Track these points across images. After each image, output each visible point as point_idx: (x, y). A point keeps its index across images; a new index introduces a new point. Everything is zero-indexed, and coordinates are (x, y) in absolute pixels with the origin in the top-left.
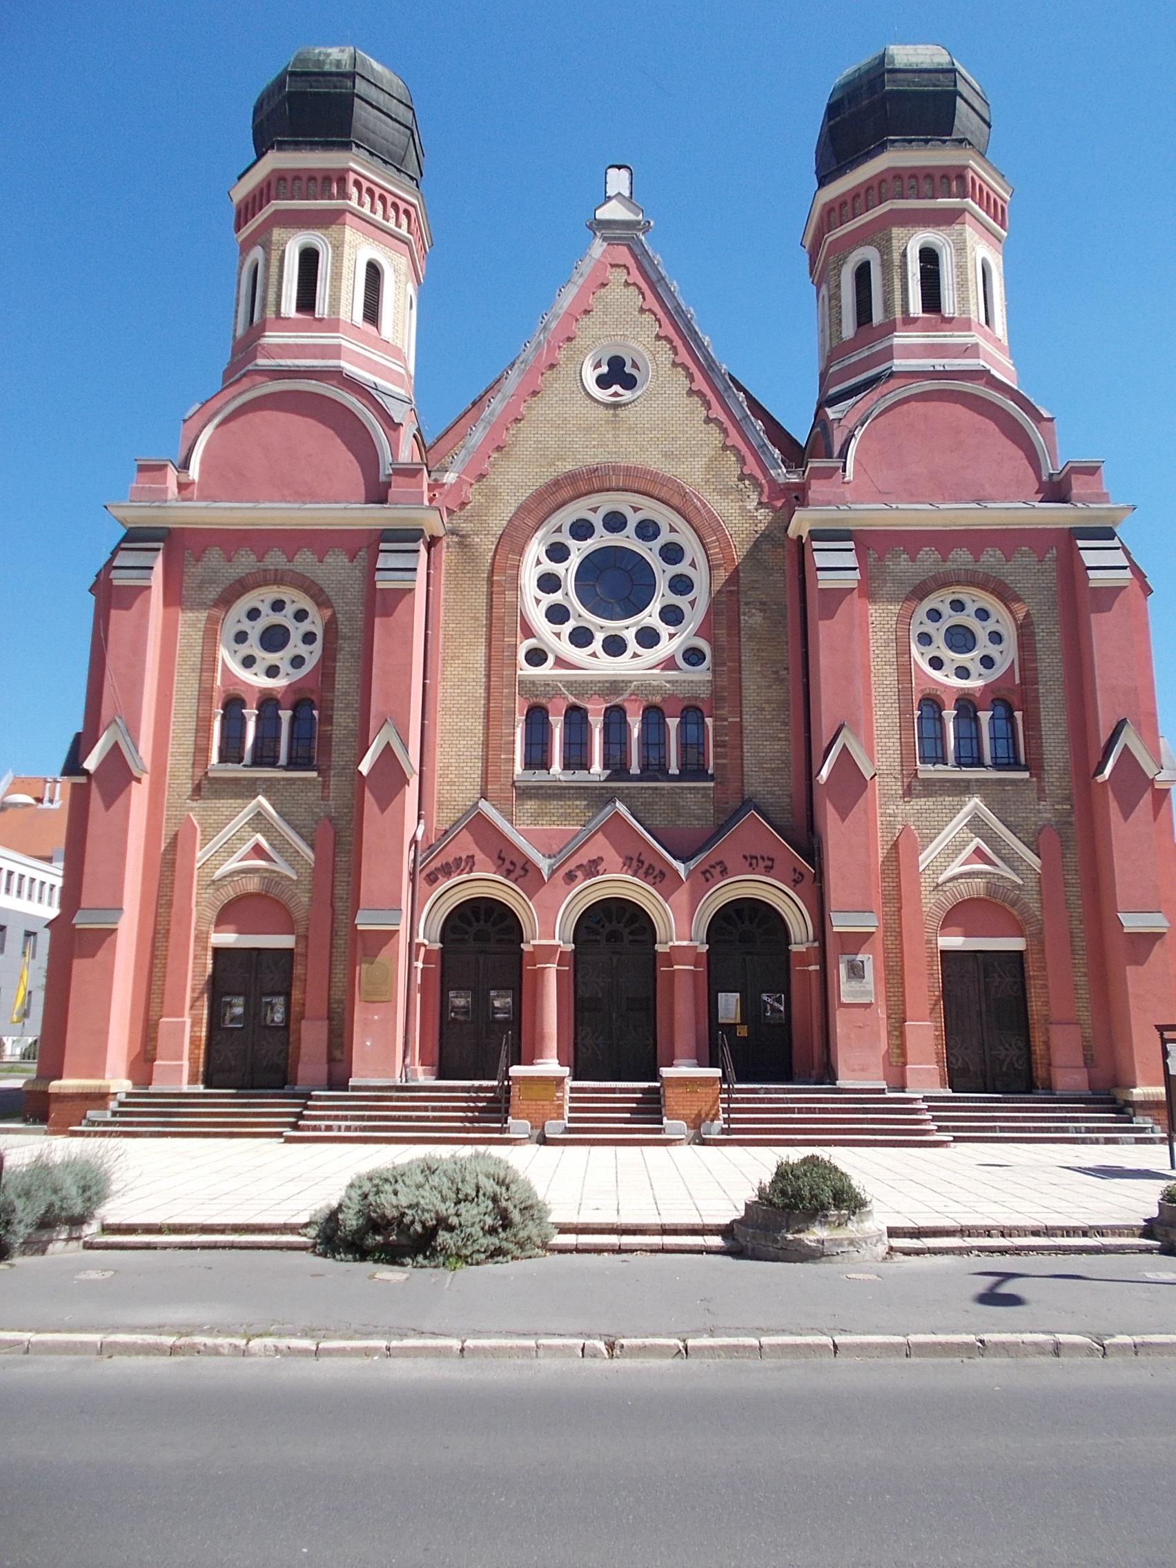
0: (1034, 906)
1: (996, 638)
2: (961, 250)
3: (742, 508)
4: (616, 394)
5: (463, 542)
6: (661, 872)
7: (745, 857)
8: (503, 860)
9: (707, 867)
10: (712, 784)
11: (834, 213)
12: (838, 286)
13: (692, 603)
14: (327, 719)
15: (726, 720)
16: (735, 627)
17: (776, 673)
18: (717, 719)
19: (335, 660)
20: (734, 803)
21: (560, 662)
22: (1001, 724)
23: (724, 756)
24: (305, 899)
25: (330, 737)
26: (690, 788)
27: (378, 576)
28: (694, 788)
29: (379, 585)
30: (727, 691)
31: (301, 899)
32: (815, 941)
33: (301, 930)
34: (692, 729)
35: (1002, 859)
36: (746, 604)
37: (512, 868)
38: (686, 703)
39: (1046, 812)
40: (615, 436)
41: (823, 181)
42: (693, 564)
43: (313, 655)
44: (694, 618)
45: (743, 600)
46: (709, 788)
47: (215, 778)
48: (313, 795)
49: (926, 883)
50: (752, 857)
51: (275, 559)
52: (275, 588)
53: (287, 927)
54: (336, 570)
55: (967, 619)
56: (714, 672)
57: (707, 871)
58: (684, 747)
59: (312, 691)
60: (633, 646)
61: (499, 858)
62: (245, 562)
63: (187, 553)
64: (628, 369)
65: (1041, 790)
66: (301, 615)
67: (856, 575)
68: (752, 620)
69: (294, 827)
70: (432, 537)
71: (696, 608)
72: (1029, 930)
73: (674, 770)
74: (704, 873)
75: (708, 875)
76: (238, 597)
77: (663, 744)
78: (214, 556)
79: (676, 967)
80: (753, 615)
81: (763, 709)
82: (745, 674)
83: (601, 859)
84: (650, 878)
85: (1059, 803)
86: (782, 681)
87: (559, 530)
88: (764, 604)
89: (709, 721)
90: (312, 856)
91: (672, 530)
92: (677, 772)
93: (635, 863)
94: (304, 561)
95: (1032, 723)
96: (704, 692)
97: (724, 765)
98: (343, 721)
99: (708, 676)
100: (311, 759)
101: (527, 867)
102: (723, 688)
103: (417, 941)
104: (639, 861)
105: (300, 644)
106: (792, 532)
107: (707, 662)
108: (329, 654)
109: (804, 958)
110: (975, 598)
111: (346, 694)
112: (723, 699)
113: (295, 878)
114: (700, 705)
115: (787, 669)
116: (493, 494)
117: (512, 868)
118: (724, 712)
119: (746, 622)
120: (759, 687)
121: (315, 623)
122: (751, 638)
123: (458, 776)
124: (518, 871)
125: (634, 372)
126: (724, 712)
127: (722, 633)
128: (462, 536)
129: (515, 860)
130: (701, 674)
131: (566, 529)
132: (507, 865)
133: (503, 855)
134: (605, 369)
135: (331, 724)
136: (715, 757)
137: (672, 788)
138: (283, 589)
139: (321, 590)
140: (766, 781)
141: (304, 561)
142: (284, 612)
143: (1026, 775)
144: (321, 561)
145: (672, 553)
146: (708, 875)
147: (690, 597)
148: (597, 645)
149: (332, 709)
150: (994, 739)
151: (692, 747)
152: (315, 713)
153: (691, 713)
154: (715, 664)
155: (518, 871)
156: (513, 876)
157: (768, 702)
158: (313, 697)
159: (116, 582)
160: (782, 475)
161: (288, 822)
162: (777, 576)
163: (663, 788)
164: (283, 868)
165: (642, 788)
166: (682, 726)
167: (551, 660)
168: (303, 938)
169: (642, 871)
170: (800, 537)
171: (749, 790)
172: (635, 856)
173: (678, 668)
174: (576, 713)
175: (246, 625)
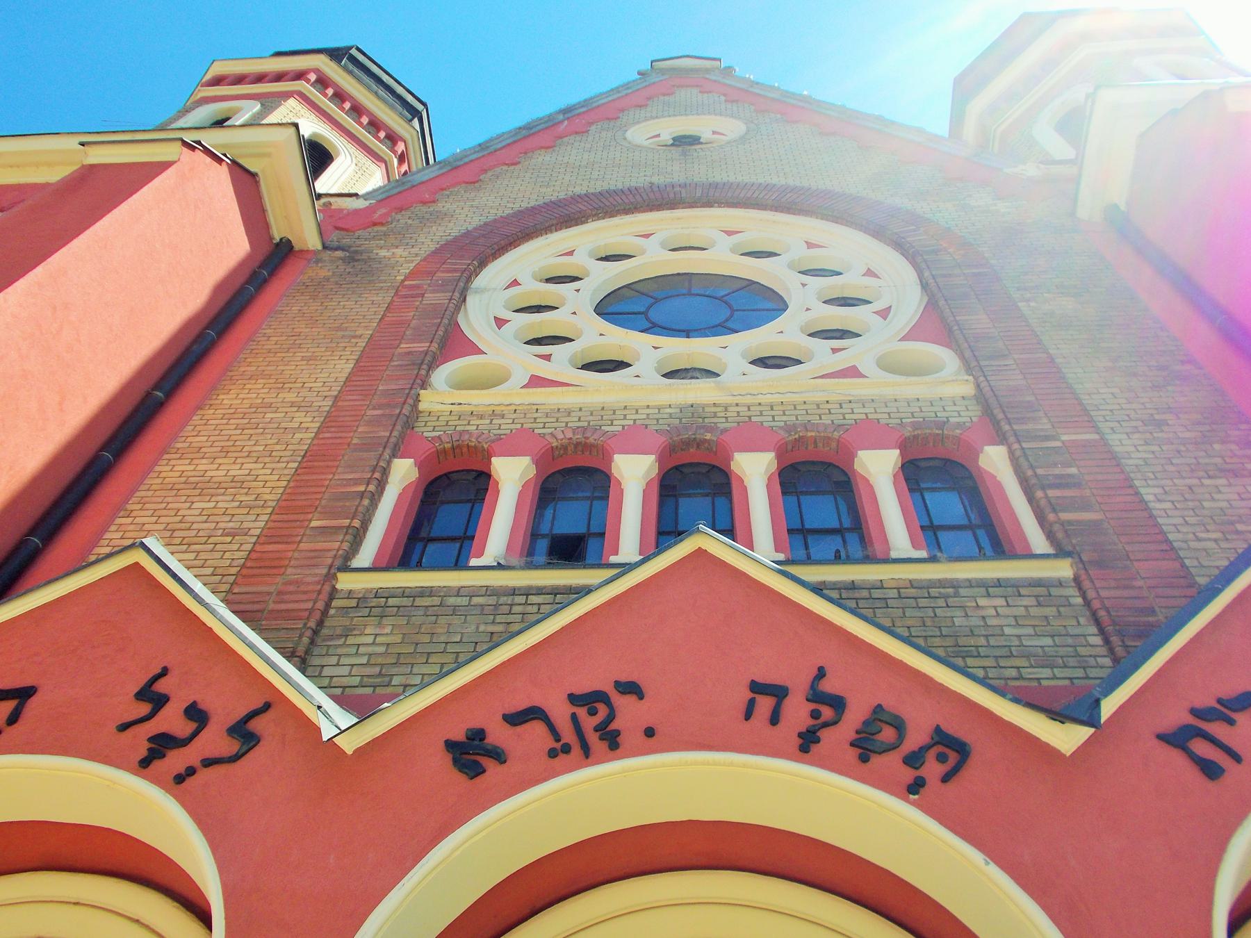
9: (1177, 716)
15: (1053, 438)
28: (999, 583)
46: (1060, 583)
83: (631, 689)
84: (891, 762)
89: (995, 461)
117: (182, 728)
124: (214, 741)
129: (208, 702)
146: (1201, 748)
156: (176, 760)
163: (880, 585)
169: (838, 737)
172: (798, 681)
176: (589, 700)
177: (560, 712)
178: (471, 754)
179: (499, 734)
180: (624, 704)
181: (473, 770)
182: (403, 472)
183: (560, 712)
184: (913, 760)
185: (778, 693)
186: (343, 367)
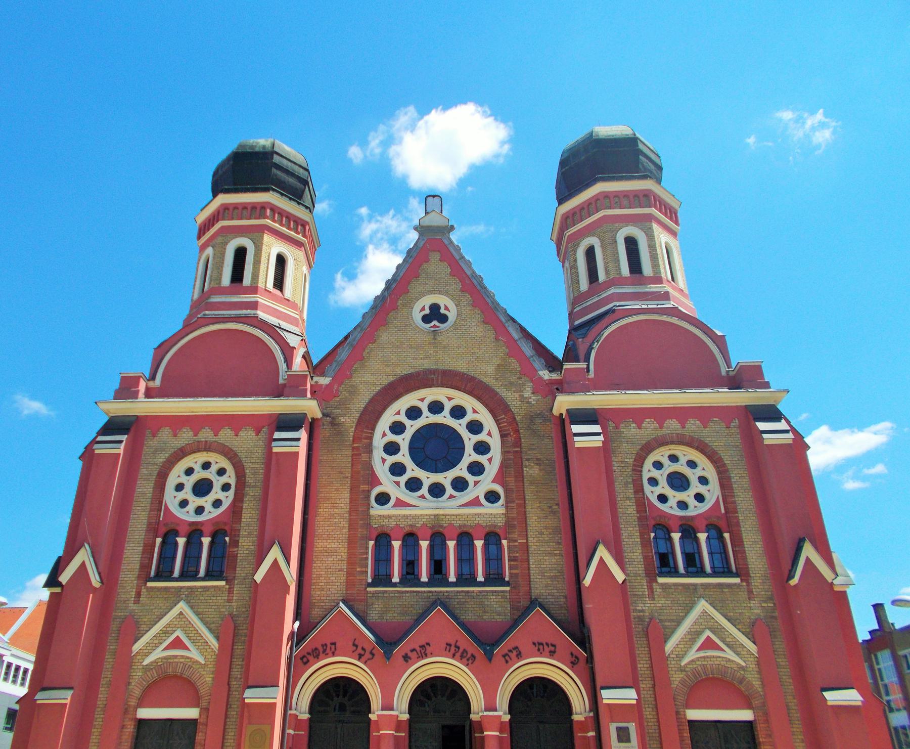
0: (757, 684)
1: (703, 480)
2: (650, 237)
3: (521, 396)
4: (435, 326)
5: (334, 423)
6: (472, 655)
7: (534, 644)
8: (357, 646)
10: (508, 588)
11: (568, 220)
12: (575, 261)
13: (490, 460)
14: (235, 543)
15: (516, 541)
16: (520, 476)
17: (550, 507)
18: (510, 540)
19: (242, 502)
20: (525, 603)
21: (400, 503)
22: (715, 542)
23: (516, 567)
24: (209, 679)
25: (237, 556)
26: (493, 592)
27: (274, 444)
28: (496, 592)
29: (275, 450)
30: (517, 520)
31: (206, 680)
32: (590, 711)
33: (204, 704)
34: (493, 548)
35: (728, 646)
36: (528, 460)
37: (362, 652)
38: (487, 529)
39: (756, 609)
40: (436, 352)
41: (561, 200)
42: (489, 434)
43: (227, 499)
44: (492, 469)
45: (525, 457)
46: (506, 591)
47: (151, 588)
48: (221, 599)
49: (672, 664)
50: (539, 644)
51: (206, 435)
52: (205, 453)
53: (194, 702)
54: (247, 442)
55: (681, 467)
56: (507, 507)
57: (507, 654)
58: (487, 560)
59: (225, 524)
60: (449, 491)
61: (354, 645)
62: (186, 436)
63: (148, 432)
64: (442, 311)
65: (750, 592)
66: (221, 472)
67: (601, 438)
68: (532, 471)
69: (206, 623)
70: (313, 419)
71: (493, 463)
72: (756, 702)
73: (480, 578)
74: (504, 656)
75: (507, 658)
76: (179, 460)
77: (472, 560)
78: (165, 433)
79: (486, 733)
80: (532, 467)
81: (541, 533)
82: (529, 508)
83: (428, 644)
84: (464, 660)
85: (765, 602)
86: (554, 513)
87: (398, 413)
88: (537, 459)
89: (504, 542)
90: (217, 645)
91: (475, 411)
92: (483, 580)
93: (453, 648)
94: (226, 435)
95: (737, 541)
96: (500, 522)
97: (517, 574)
98: (246, 544)
99: (503, 510)
100: (222, 572)
101: (374, 651)
102: (513, 519)
103: (290, 712)
104: (456, 646)
105: (220, 491)
106: (556, 412)
107: (502, 501)
108: (239, 498)
109: (583, 725)
110: (686, 453)
111: (248, 525)
112: (514, 526)
113: (203, 662)
114: (498, 531)
115: (557, 504)
116: (354, 391)
117: (362, 652)
118: (515, 536)
119: (528, 472)
120: (539, 518)
121: (230, 478)
122: (531, 483)
123: (327, 583)
124: (368, 655)
125: (446, 312)
126: (515, 536)
127: (511, 480)
128: (333, 418)
129: (365, 647)
130: (497, 509)
131: (403, 412)
132: (360, 650)
133: (356, 643)
134: (427, 311)
135: (237, 546)
136: (510, 568)
137: (480, 592)
138: (210, 454)
139: (236, 455)
140: (547, 586)
141: (226, 435)
142: (209, 470)
143: (737, 580)
144: (236, 435)
145: (475, 427)
147: (488, 456)
148: (424, 490)
149: (239, 536)
150: (711, 553)
151: (493, 560)
152: (227, 539)
153: (492, 537)
154: (507, 502)
155: (368, 655)
156: (364, 658)
157: (546, 528)
158: (226, 528)
159: (97, 452)
160: (545, 375)
161: (202, 620)
162: (546, 441)
163: (473, 592)
164: (194, 654)
165: (458, 592)
166: (486, 546)
167: (393, 501)
168: (205, 711)
169: (458, 655)
170: (561, 415)
171: (535, 592)
172: (453, 642)
173: (481, 505)
174: (411, 538)
175: (184, 479)
176: (422, 647)
177: (418, 649)
178: (406, 658)
179: (410, 654)
180: (427, 647)
181: (407, 661)
182: (371, 543)
183: (418, 649)
184: (468, 660)
185: (450, 645)
186: (347, 495)
